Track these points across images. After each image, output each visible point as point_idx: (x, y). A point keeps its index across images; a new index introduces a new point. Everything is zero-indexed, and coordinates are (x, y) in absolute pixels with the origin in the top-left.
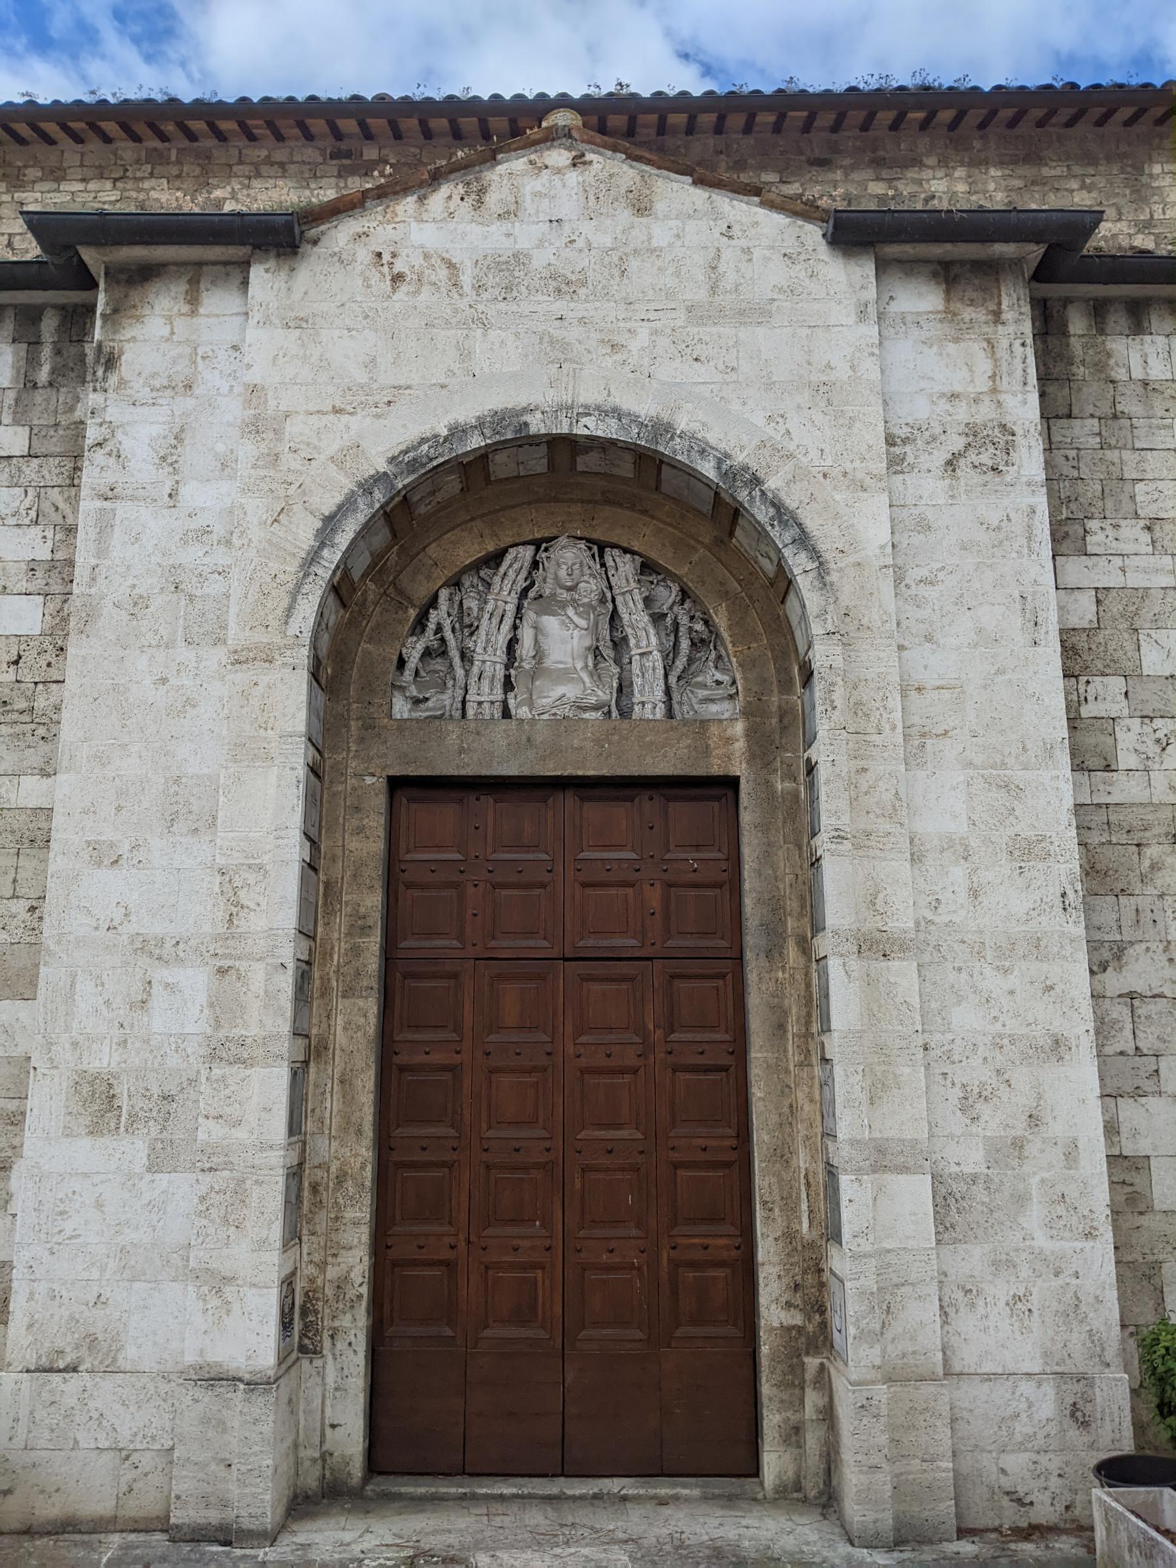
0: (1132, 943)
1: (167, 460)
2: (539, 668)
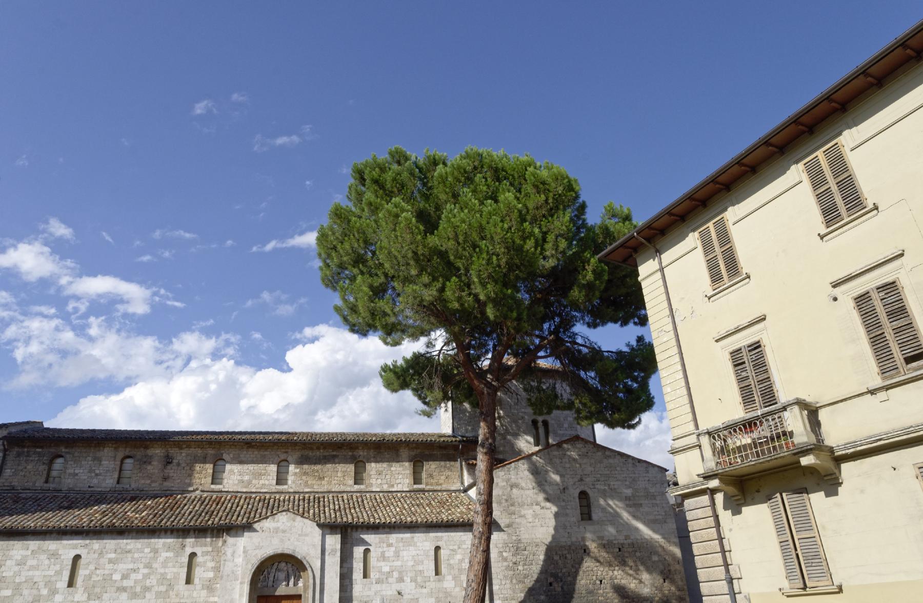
1: (233, 556)
2: (277, 580)
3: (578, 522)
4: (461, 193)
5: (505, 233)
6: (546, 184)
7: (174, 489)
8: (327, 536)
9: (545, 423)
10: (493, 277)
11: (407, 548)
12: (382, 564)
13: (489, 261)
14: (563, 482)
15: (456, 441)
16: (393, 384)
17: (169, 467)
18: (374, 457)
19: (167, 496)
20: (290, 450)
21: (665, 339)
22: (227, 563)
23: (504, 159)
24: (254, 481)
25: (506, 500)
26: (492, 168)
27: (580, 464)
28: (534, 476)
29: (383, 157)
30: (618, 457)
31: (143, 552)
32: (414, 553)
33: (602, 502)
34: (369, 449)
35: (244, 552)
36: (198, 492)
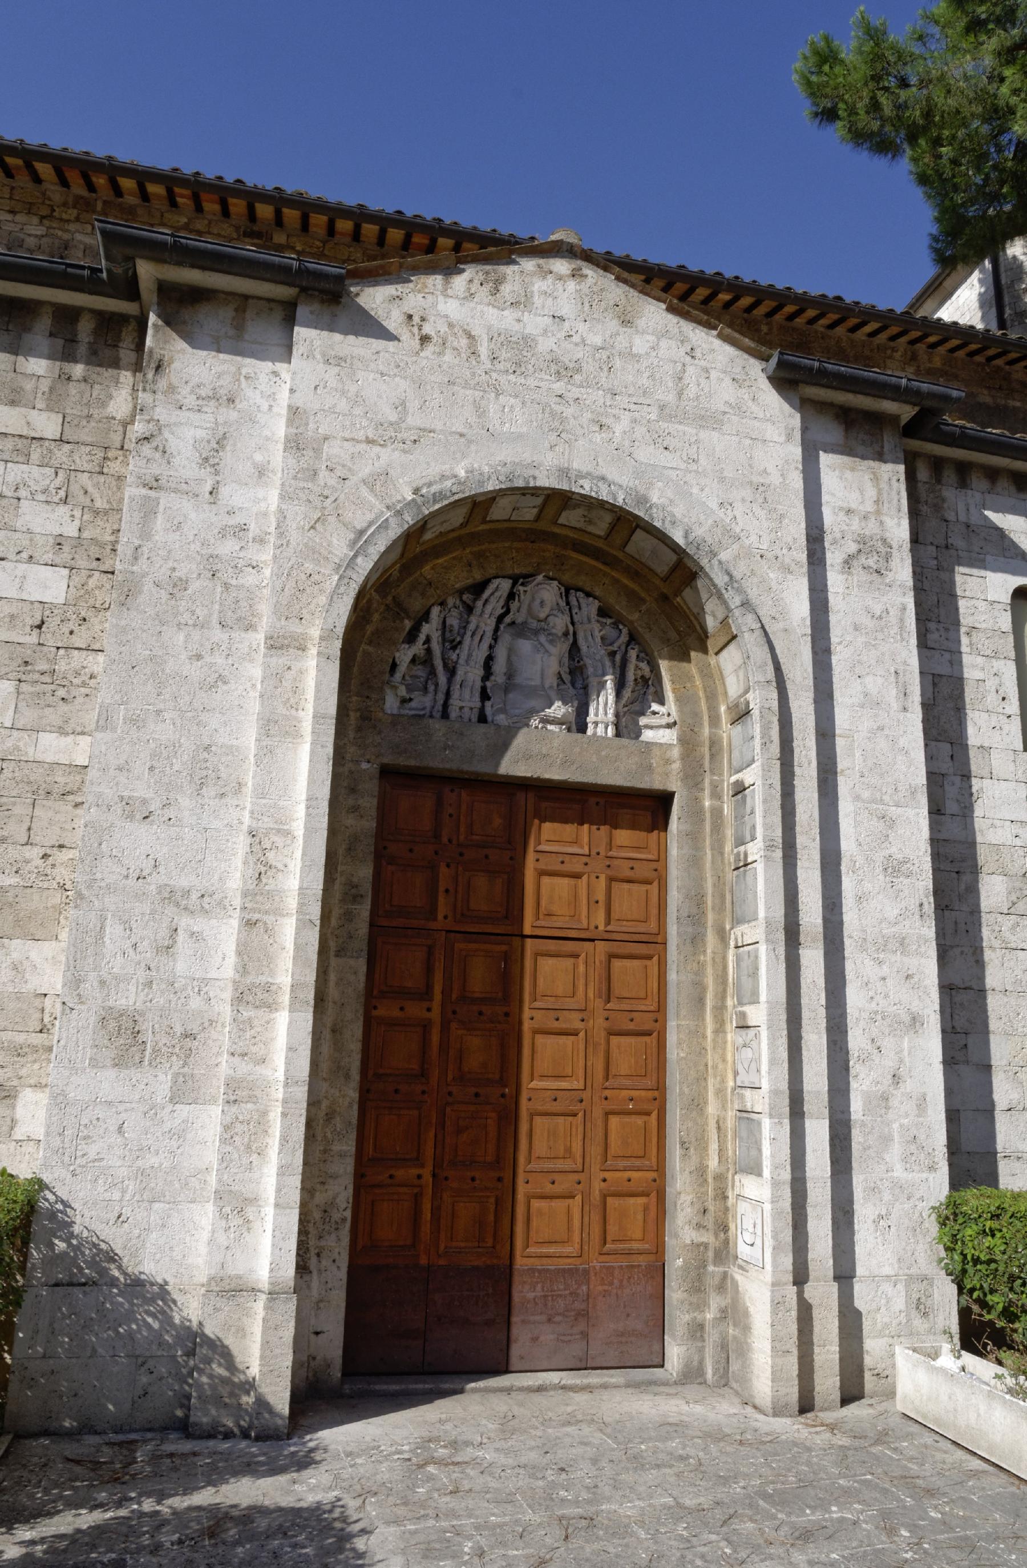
0: (952, 947)
2: (510, 685)
8: (825, 459)
35: (295, 444)
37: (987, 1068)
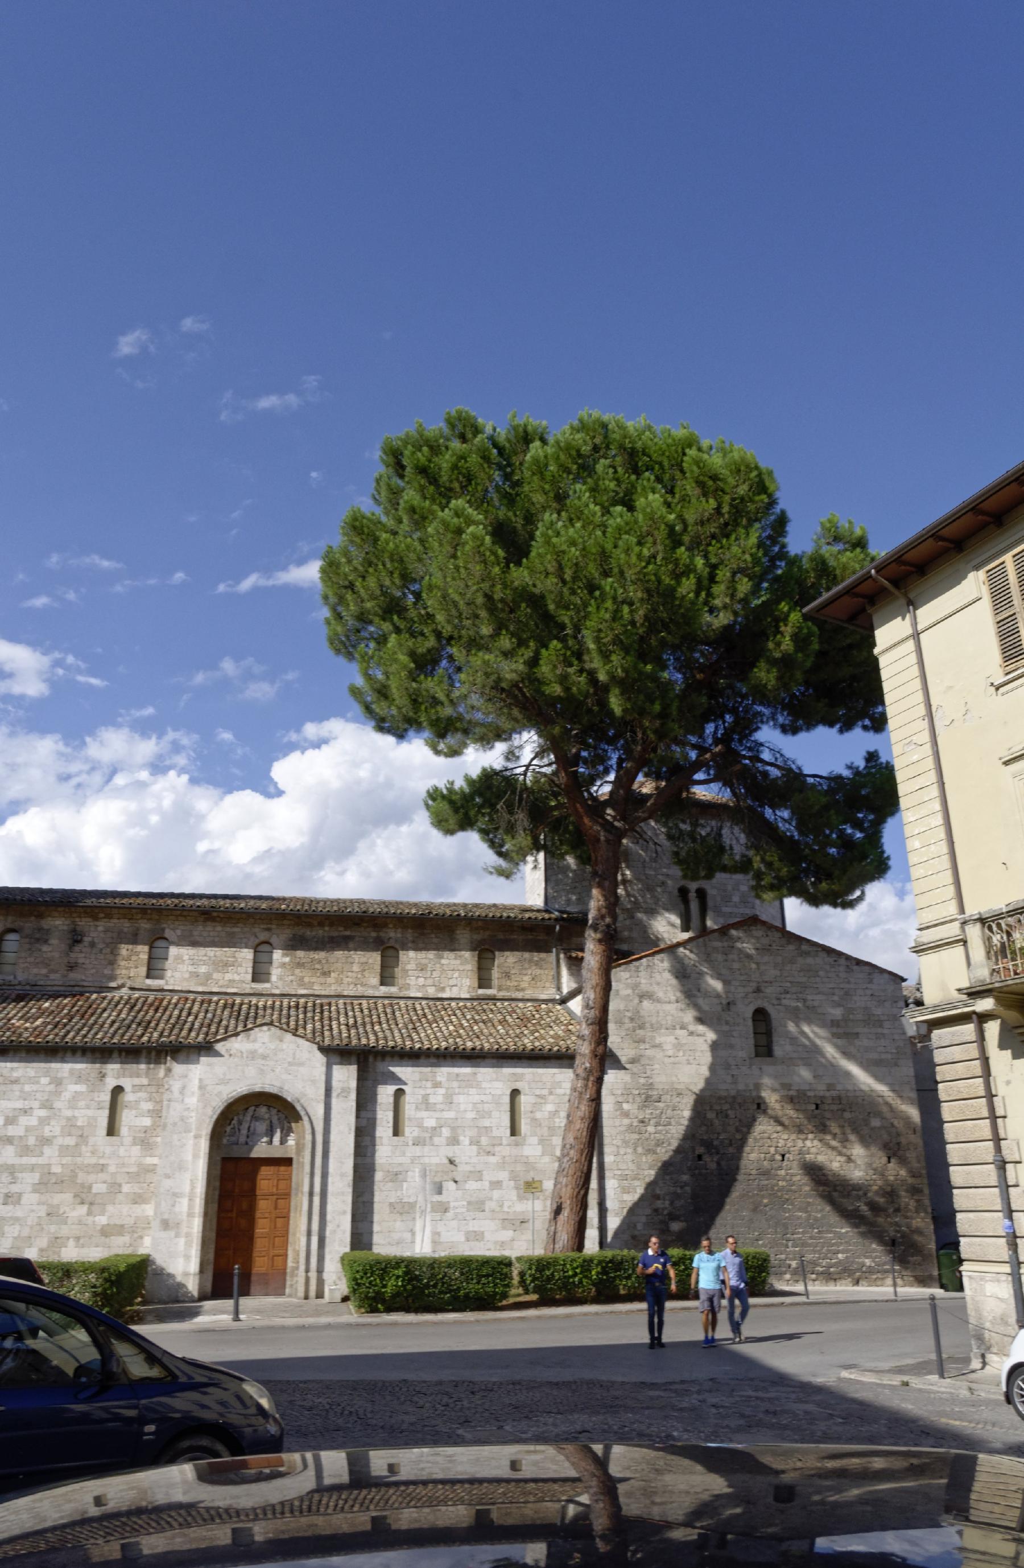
2: (254, 1134)
3: (751, 1058)
4: (571, 493)
5: (643, 564)
6: (719, 479)
7: (85, 984)
8: (335, 1067)
9: (701, 894)
10: (621, 642)
11: (466, 1090)
12: (424, 1114)
13: (616, 616)
14: (727, 992)
15: (550, 919)
16: (447, 821)
17: (77, 948)
18: (413, 942)
19: (74, 996)
20: (274, 926)
21: (915, 758)
22: (172, 1104)
23: (647, 433)
24: (215, 976)
25: (632, 1019)
26: (625, 449)
27: (757, 964)
28: (680, 981)
29: (436, 426)
30: (823, 955)
31: (38, 1083)
32: (477, 1098)
33: (791, 1027)
34: (405, 928)
35: (201, 1088)
36: (124, 991)
37: (372, 1222)
